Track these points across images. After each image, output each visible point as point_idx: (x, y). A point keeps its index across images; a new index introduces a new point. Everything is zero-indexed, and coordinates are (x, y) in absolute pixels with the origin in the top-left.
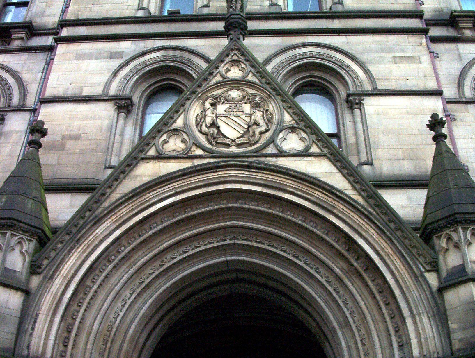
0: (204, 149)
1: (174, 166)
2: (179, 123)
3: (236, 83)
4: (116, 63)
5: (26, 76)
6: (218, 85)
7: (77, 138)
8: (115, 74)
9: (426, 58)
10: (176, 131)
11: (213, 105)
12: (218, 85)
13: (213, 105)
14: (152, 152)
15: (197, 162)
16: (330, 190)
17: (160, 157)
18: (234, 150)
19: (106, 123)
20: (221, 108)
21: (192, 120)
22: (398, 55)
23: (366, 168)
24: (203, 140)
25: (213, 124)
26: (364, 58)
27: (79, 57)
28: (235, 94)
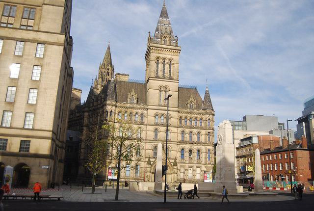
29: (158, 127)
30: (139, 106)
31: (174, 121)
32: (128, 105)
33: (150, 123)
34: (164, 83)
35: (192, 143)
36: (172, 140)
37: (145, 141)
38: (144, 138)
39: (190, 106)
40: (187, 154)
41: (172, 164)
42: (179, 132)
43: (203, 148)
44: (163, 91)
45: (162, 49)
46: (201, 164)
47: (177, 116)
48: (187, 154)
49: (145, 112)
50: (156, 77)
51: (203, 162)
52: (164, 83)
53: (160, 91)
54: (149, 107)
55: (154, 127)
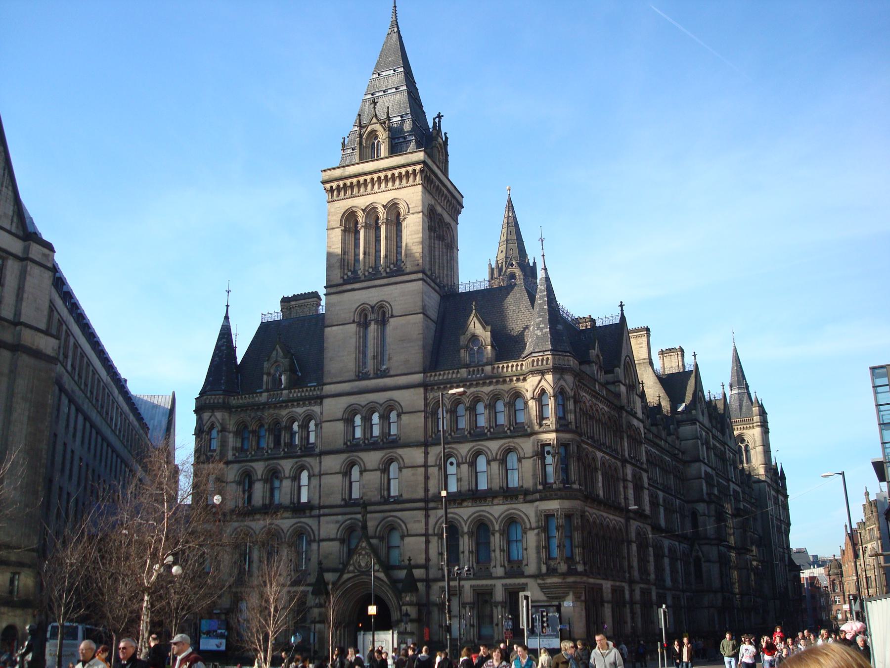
0: (357, 570)
1: (351, 575)
2: (352, 562)
3: (364, 549)
4: (338, 525)
5: (314, 528)
6: (360, 549)
7: (331, 554)
8: (338, 530)
9: (423, 521)
10: (351, 565)
11: (359, 556)
12: (360, 549)
13: (359, 556)
14: (346, 571)
15: (357, 574)
16: (382, 580)
17: (349, 572)
18: (364, 570)
19: (338, 548)
20: (361, 557)
21: (355, 560)
22: (416, 519)
23: (403, 563)
24: (357, 567)
25: (359, 562)
26: (406, 521)
27: (327, 522)
28: (364, 552)
29: (355, 456)
30: (296, 393)
31: (414, 425)
32: (264, 397)
33: (328, 448)
34: (371, 296)
35: (475, 496)
36: (405, 496)
37: (316, 512)
38: (316, 502)
39: (472, 355)
40: (466, 544)
41: (400, 586)
42: (431, 460)
43: (529, 511)
44: (371, 320)
45: (362, 179)
46: (522, 575)
47: (420, 404)
48: (466, 544)
49: (317, 409)
50: (346, 282)
51: (531, 569)
52: (371, 296)
53: (364, 324)
54: (328, 389)
55: (343, 456)
